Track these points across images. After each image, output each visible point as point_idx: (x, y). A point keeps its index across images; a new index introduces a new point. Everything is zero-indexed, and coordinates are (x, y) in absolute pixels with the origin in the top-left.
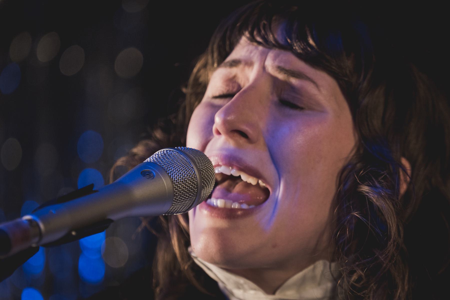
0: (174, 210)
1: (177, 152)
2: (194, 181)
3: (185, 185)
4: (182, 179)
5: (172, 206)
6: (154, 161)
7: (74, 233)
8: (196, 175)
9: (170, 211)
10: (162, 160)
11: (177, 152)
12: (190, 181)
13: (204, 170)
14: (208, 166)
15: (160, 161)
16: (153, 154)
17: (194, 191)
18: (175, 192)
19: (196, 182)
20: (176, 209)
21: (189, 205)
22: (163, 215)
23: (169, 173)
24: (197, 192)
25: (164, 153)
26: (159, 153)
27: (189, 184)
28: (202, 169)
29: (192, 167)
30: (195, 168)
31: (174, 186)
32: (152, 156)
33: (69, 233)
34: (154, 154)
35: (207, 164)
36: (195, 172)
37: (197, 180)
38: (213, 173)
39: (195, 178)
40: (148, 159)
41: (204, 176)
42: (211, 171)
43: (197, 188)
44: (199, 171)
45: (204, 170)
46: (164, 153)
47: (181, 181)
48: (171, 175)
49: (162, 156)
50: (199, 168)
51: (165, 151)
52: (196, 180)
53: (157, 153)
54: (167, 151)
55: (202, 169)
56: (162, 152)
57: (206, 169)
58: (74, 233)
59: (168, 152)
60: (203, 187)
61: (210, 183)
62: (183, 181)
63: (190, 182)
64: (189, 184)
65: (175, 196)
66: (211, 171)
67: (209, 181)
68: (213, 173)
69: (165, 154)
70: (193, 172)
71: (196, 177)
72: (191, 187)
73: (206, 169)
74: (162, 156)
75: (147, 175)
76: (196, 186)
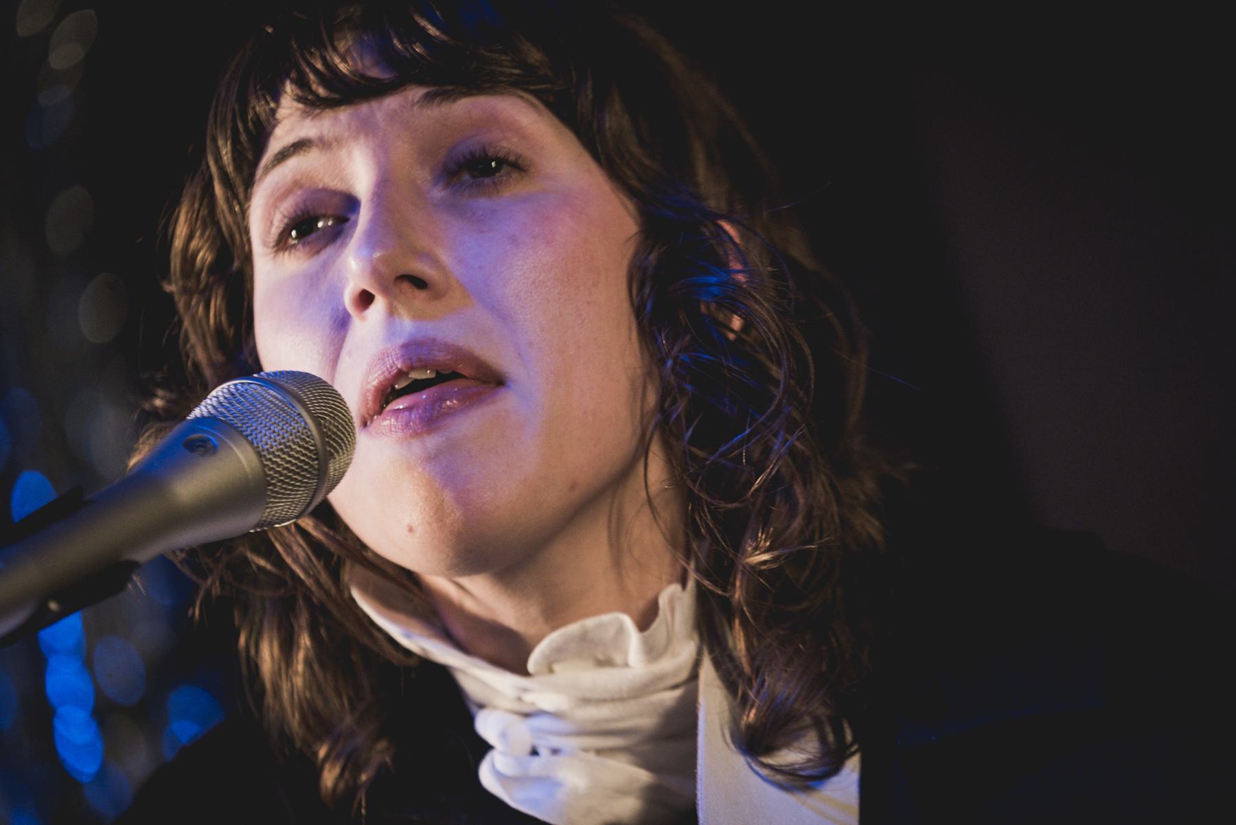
0: (274, 516)
1: (259, 385)
2: (307, 443)
3: (290, 456)
4: (280, 444)
5: (267, 508)
6: (209, 412)
7: (53, 606)
8: (310, 431)
9: (265, 521)
10: (226, 408)
11: (259, 385)
12: (300, 446)
13: (326, 414)
14: (334, 404)
15: (223, 410)
16: (205, 398)
17: (312, 466)
18: (268, 475)
19: (312, 446)
20: (277, 513)
21: (305, 500)
22: (252, 531)
23: (247, 436)
24: (318, 470)
25: (229, 391)
26: (220, 393)
27: (298, 452)
28: (321, 413)
29: (299, 414)
30: (304, 414)
31: (266, 463)
32: (203, 403)
33: (43, 607)
34: (209, 397)
35: (331, 400)
36: (306, 423)
37: (313, 440)
38: (349, 420)
39: (308, 437)
40: (197, 412)
41: (330, 430)
42: (343, 415)
43: (317, 459)
44: (316, 419)
45: (326, 414)
46: (229, 391)
47: (278, 450)
48: (252, 440)
49: (226, 398)
50: (315, 413)
51: (232, 387)
52: (312, 441)
53: (214, 393)
54: (235, 385)
55: (321, 413)
56: (225, 391)
57: (331, 412)
58: (53, 606)
59: (239, 387)
60: (332, 455)
61: (344, 443)
62: (282, 450)
63: (299, 449)
64: (298, 452)
65: (269, 486)
66: (343, 415)
67: (341, 439)
68: (349, 420)
69: (232, 394)
70: (303, 424)
71: (312, 435)
72: (302, 458)
73: (331, 412)
74: (226, 398)
75: (199, 446)
76: (315, 455)
